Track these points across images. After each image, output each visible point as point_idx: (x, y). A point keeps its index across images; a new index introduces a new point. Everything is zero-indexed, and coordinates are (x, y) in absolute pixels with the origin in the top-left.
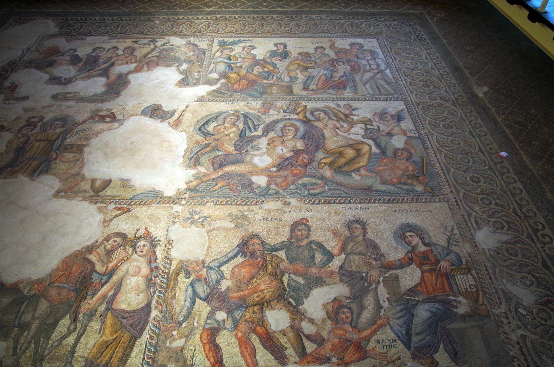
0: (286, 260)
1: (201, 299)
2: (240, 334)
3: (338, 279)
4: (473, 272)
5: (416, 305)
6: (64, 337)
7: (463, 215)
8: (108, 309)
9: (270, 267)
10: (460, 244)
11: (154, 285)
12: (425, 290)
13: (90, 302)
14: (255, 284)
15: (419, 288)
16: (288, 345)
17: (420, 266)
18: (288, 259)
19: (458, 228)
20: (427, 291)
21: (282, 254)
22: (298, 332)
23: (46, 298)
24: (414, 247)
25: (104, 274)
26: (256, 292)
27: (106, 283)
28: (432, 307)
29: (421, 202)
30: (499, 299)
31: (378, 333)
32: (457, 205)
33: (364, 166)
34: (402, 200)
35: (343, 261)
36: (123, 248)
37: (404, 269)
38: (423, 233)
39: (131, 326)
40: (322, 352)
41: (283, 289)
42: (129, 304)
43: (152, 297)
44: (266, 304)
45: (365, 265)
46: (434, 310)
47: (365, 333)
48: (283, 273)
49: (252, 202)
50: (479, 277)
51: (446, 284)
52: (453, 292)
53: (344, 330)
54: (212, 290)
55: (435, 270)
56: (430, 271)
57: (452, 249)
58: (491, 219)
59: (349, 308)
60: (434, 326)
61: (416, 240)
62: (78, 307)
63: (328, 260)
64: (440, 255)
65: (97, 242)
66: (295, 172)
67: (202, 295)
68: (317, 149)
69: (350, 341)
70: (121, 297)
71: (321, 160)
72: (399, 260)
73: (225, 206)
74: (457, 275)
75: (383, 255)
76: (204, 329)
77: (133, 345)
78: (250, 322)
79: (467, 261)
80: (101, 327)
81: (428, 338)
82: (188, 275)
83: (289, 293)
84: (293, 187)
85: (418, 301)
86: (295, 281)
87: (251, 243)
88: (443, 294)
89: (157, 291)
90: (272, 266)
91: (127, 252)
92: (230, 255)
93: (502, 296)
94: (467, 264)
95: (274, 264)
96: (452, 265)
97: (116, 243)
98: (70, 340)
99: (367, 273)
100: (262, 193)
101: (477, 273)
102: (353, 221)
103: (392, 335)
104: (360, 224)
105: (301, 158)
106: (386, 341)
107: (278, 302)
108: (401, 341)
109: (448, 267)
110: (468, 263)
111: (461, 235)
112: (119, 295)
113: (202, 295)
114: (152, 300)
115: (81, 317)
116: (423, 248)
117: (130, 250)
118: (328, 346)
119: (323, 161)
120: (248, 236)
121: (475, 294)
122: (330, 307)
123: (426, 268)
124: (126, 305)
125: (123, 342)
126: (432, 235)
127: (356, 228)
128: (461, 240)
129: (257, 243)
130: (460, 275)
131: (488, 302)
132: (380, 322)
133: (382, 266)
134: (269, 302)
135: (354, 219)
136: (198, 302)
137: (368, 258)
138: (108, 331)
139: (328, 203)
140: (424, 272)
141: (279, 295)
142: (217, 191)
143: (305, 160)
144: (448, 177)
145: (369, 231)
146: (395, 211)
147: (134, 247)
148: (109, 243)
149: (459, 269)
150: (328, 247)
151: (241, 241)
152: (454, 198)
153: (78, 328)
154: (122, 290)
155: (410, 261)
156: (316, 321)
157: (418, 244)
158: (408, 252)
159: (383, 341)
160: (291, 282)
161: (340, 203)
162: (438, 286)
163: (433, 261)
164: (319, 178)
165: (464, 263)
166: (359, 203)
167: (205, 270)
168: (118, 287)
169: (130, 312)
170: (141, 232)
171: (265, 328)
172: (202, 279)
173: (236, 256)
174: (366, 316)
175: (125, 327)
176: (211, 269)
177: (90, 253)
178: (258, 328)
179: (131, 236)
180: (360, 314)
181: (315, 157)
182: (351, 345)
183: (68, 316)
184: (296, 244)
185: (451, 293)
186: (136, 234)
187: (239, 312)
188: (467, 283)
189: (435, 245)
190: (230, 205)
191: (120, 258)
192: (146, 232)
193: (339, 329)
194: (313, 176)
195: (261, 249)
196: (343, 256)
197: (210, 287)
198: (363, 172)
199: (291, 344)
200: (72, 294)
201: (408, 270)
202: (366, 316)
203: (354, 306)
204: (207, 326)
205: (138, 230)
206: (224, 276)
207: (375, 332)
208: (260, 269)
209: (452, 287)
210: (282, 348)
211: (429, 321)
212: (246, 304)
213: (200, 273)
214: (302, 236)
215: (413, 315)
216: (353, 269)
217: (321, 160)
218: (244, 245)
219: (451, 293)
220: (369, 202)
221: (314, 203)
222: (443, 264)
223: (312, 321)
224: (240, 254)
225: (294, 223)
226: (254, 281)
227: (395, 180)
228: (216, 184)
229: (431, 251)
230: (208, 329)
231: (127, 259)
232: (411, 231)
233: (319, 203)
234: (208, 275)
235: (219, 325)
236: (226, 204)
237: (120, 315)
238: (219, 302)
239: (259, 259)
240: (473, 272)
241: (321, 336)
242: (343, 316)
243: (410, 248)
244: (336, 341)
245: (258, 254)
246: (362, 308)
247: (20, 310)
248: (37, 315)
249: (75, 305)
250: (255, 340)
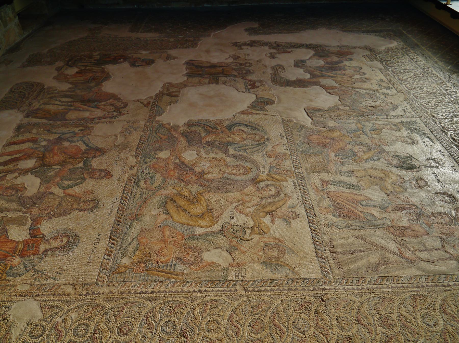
17: (26, 242)
22: (11, 172)
58: (50, 325)
79: (9, 281)
96: (11, 267)
99: (38, 207)
109: (11, 263)
111: (42, 285)
116: (42, 248)
142: (157, 136)
156: (15, 179)
157: (50, 245)
158: (44, 236)
165: (7, 278)
189: (42, 259)
203: (13, 198)
210: (6, 165)
223: (16, 178)
242: (10, 191)
243: (47, 238)
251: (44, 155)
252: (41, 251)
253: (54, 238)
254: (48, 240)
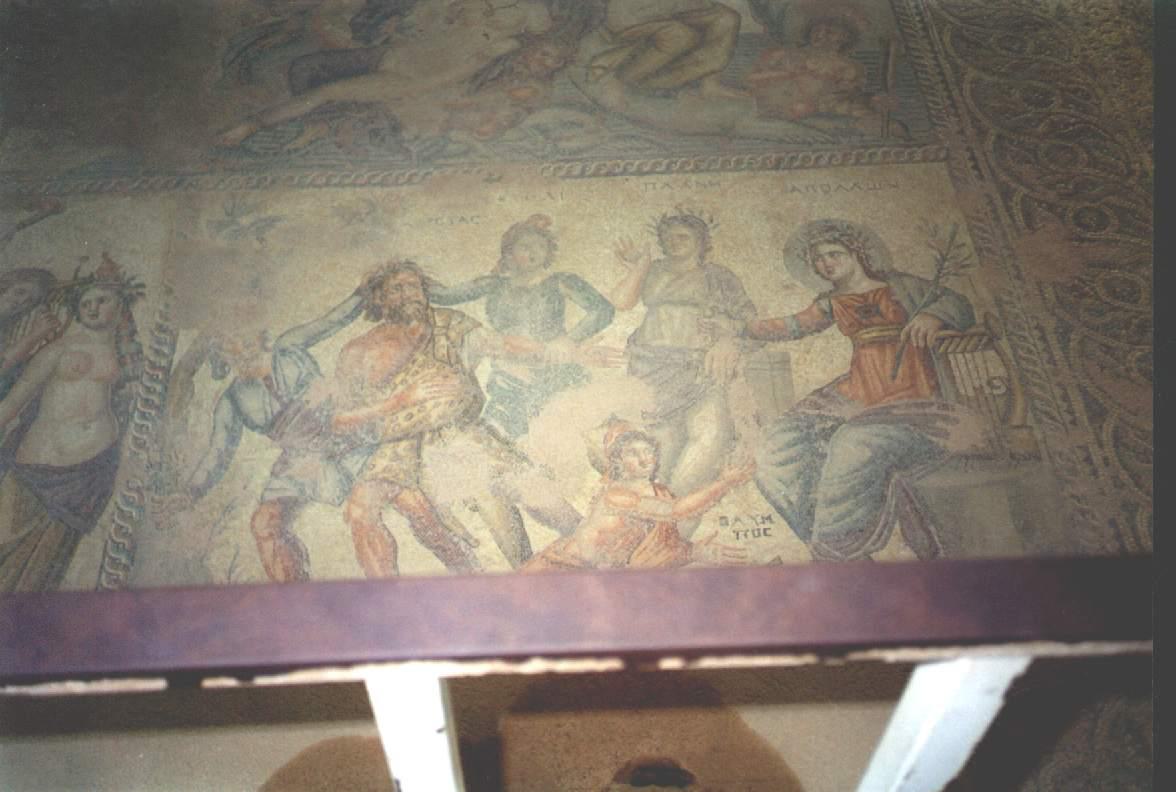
0: (486, 324)
1: (254, 427)
2: (357, 512)
3: (624, 367)
4: (1004, 344)
5: (833, 429)
7: (988, 196)
9: (443, 341)
10: (971, 271)
12: (861, 393)
14: (400, 388)
15: (845, 387)
16: (484, 534)
17: (851, 330)
18: (491, 321)
19: (970, 230)
20: (868, 395)
21: (477, 309)
24: (836, 284)
26: (404, 408)
28: (877, 435)
29: (869, 163)
30: (1071, 412)
31: (724, 500)
32: (975, 167)
33: (713, 72)
34: (817, 159)
35: (638, 324)
37: (808, 339)
38: (869, 244)
40: (574, 549)
41: (475, 397)
44: (428, 436)
45: (699, 331)
46: (884, 442)
47: (690, 501)
48: (477, 357)
49: (397, 178)
50: (1018, 358)
51: (923, 376)
52: (940, 395)
53: (635, 494)
54: (286, 407)
55: (893, 341)
56: (880, 343)
57: (947, 285)
59: (650, 441)
60: (878, 482)
61: (845, 265)
63: (598, 320)
64: (912, 301)
66: (523, 93)
67: (259, 418)
68: (586, 27)
69: (648, 521)
71: (594, 58)
72: (794, 316)
73: (325, 189)
74: (954, 352)
75: (750, 305)
76: (262, 504)
78: (385, 480)
79: (986, 316)
81: (860, 513)
82: (220, 372)
83: (491, 406)
84: (510, 134)
85: (840, 421)
86: (509, 377)
87: (393, 282)
88: (911, 401)
90: (448, 338)
92: (335, 316)
93: (1079, 406)
94: (986, 323)
95: (453, 334)
99: (704, 351)
100: (425, 154)
101: (1014, 348)
102: (675, 218)
103: (765, 508)
104: (691, 226)
105: (538, 55)
106: (745, 519)
107: (462, 429)
108: (786, 518)
109: (930, 333)
110: (992, 322)
111: (979, 250)
113: (259, 418)
116: (863, 285)
118: (587, 535)
119: (601, 62)
120: (385, 265)
121: (1001, 402)
122: (597, 437)
123: (867, 335)
126: (893, 249)
127: (681, 236)
128: (975, 259)
129: (410, 284)
130: (963, 352)
131: (1039, 421)
132: (728, 474)
133: (747, 333)
134: (437, 431)
135: (676, 213)
136: (250, 439)
137: (709, 313)
139: (608, 174)
140: (863, 346)
141: (466, 412)
143: (549, 62)
144: (955, 93)
145: (716, 244)
146: (794, 189)
149: (962, 338)
150: (600, 289)
151: (365, 281)
152: (968, 149)
155: (827, 319)
157: (852, 273)
159: (737, 519)
160: (499, 379)
161: (640, 173)
162: (898, 381)
163: (891, 316)
164: (584, 108)
165: (979, 320)
166: (693, 171)
167: (266, 359)
171: (424, 494)
172: (260, 380)
173: (351, 317)
174: (693, 458)
176: (283, 352)
178: (408, 497)
180: (677, 453)
181: (577, 51)
182: (649, 530)
184: (516, 283)
185: (933, 399)
187: (356, 457)
188: (982, 372)
189: (901, 275)
190: (336, 185)
193: (618, 490)
194: (567, 104)
195: (421, 297)
196: (640, 308)
197: (279, 398)
198: (710, 87)
199: (492, 530)
201: (818, 342)
202: (693, 458)
203: (662, 434)
204: (269, 496)
206: (317, 370)
207: (716, 497)
208: (416, 348)
209: (937, 383)
211: (866, 471)
212: (374, 438)
213: (255, 364)
214: (532, 260)
215: (823, 456)
216: (667, 342)
217: (594, 58)
218: (374, 289)
219: (933, 399)
220: (723, 168)
221: (568, 175)
222: (921, 325)
224: (364, 313)
225: (512, 228)
226: (398, 379)
227: (800, 107)
228: (300, 133)
229: (887, 292)
230: (273, 503)
232: (835, 241)
233: (582, 175)
234: (275, 368)
235: (302, 491)
236: (327, 184)
238: (303, 434)
239: (414, 323)
240: (1004, 344)
241: (573, 510)
242: (633, 460)
243: (827, 286)
244: (610, 521)
245: (410, 309)
246: (684, 439)
250: (397, 524)
251: (406, 436)
252: (882, 285)
253: (826, 274)
254: (836, 284)
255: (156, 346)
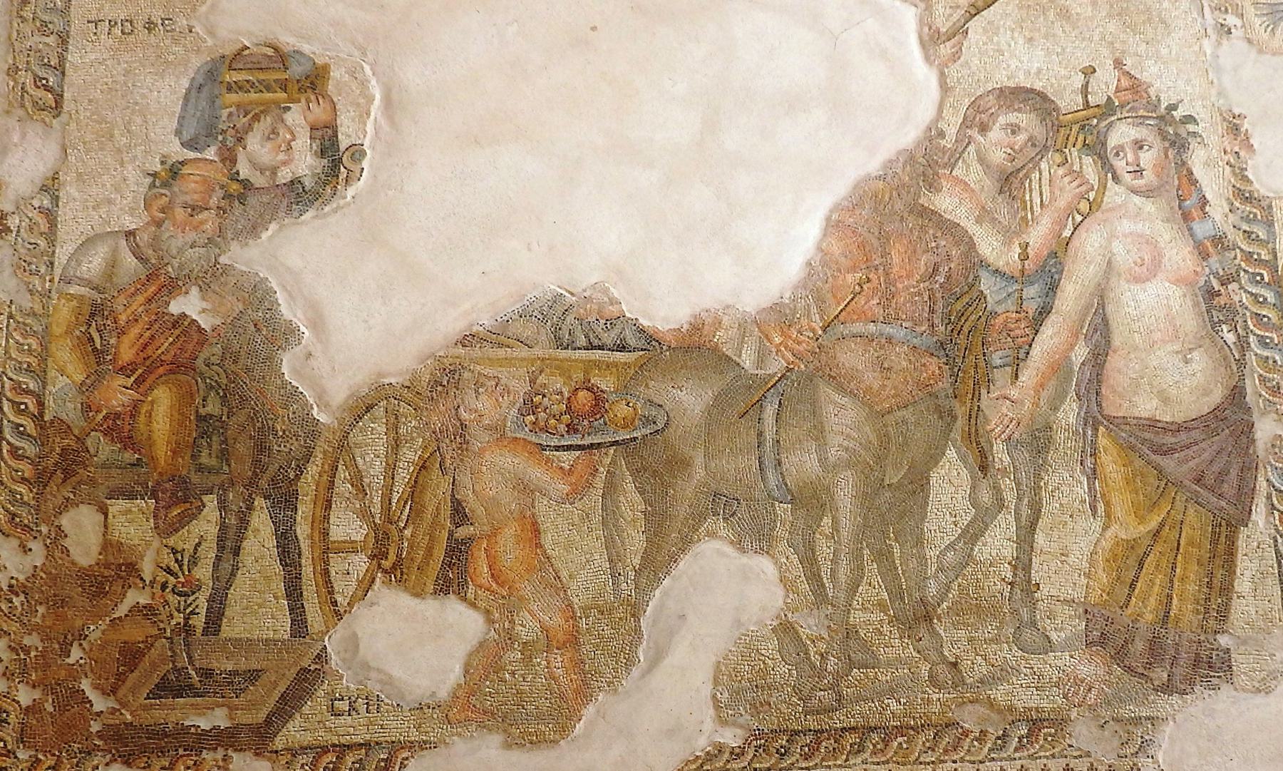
6: (973, 534)
8: (1094, 419)
11: (1231, 314)
13: (1014, 393)
23: (839, 382)
25: (1024, 278)
27: (1044, 312)
36: (1058, 158)
39: (1198, 481)
42: (1165, 400)
43: (1241, 363)
62: (975, 415)
65: (941, 134)
70: (1120, 369)
77: (1231, 553)
80: (1091, 488)
89: (1252, 338)
91: (1080, 174)
97: (1021, 138)
98: (998, 542)
112: (1114, 362)
114: (1242, 378)
115: (1000, 455)
117: (1089, 168)
124: (1155, 402)
125: (1191, 543)
138: (1121, 503)
147: (1097, 149)
148: (991, 135)
153: (1010, 496)
154: (1117, 341)
168: (1098, 329)
169: (1177, 428)
170: (1105, 85)
175: (1179, 485)
177: (933, 186)
179: (1068, 101)
183: (951, 453)
186: (1085, 90)
191: (1062, 203)
192: (1125, 83)
200: (933, 365)
205: (1089, 71)
231: (1089, 207)
237: (1144, 441)
247: (760, 434)
248: (833, 454)
249: (961, 411)
255: (1245, 227)
